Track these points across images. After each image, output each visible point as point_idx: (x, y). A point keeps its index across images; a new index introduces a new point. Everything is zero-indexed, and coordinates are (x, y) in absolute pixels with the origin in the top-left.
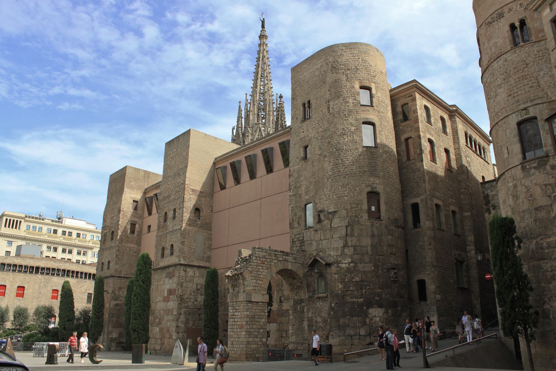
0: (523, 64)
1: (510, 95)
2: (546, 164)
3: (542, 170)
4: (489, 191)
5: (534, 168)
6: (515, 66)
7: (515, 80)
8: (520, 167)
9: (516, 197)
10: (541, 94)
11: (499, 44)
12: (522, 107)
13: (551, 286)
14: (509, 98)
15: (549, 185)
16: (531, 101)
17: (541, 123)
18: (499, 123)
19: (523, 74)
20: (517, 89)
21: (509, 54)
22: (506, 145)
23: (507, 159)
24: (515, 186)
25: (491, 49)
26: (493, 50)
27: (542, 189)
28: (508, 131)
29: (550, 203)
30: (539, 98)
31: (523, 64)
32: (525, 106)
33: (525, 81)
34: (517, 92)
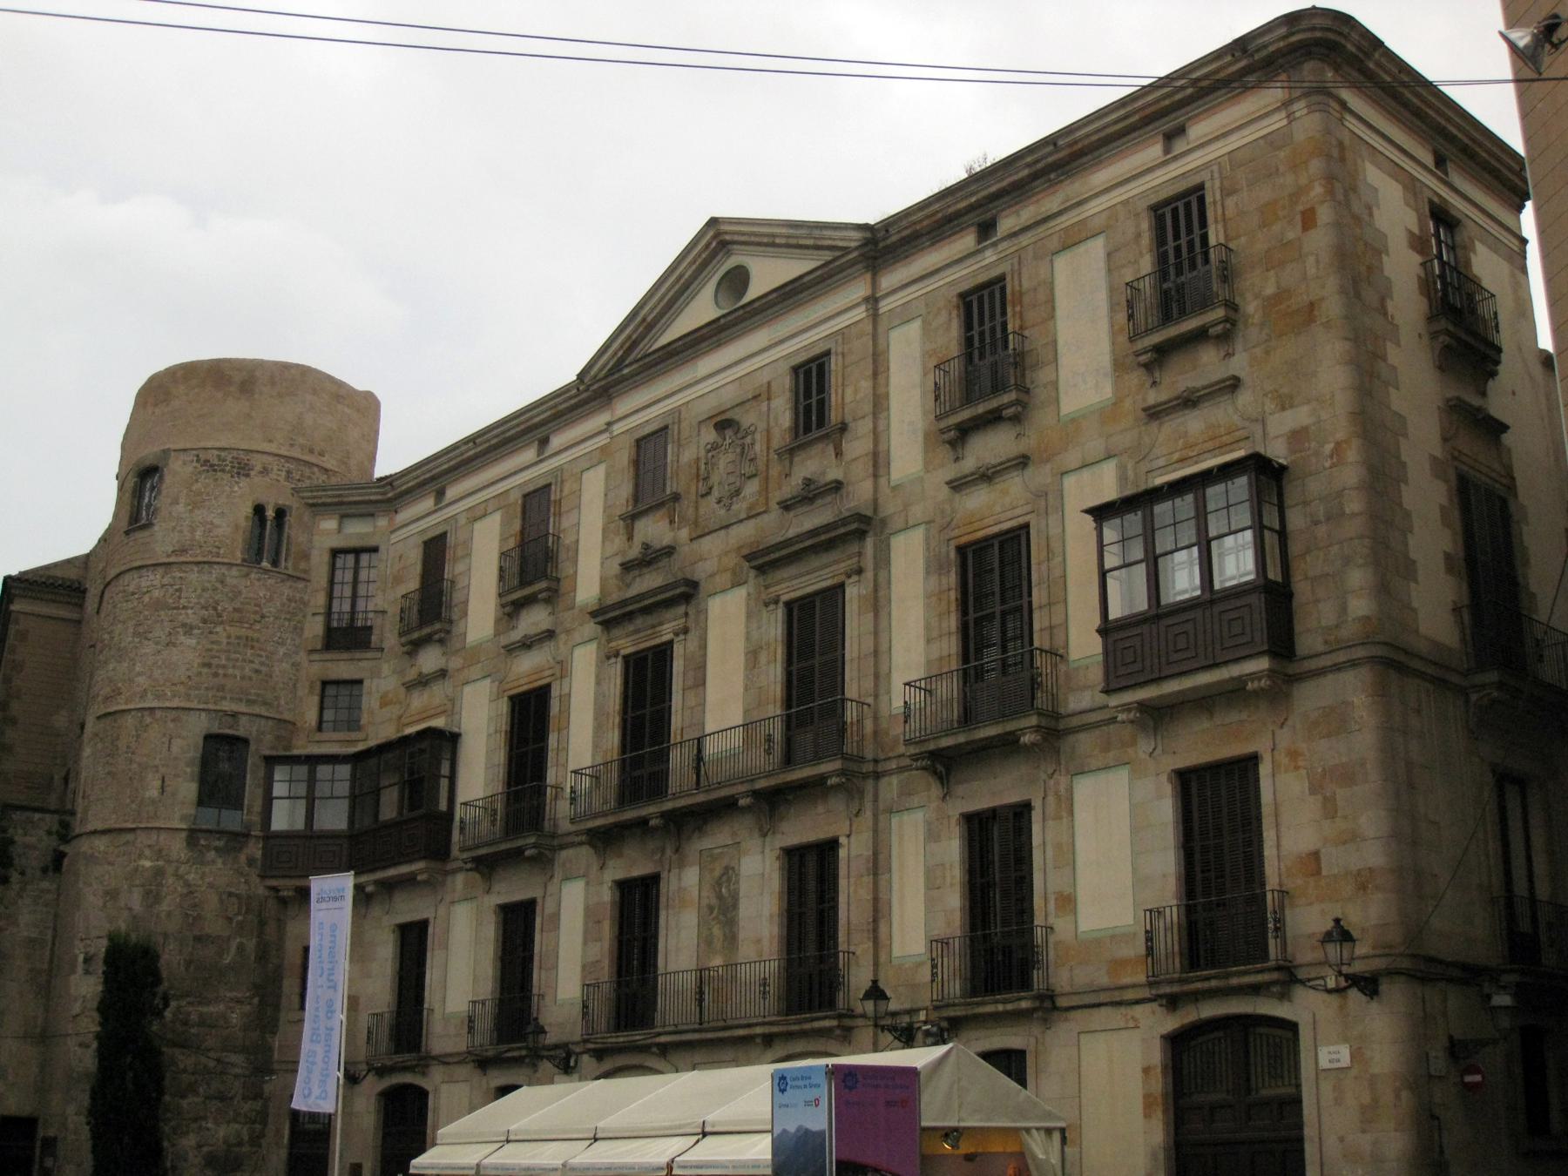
0: (255, 613)
1: (209, 665)
4: (20, 831)
6: (238, 605)
7: (229, 637)
8: (184, 835)
9: (152, 897)
11: (219, 531)
12: (227, 706)
13: (184, 1103)
14: (205, 670)
15: (238, 896)
16: (250, 702)
17: (252, 760)
19: (250, 633)
20: (228, 659)
21: (234, 571)
22: (162, 770)
23: (153, 802)
24: (159, 873)
25: (193, 531)
26: (198, 534)
27: (221, 901)
30: (265, 703)
31: (255, 613)
32: (234, 707)
33: (249, 652)
34: (224, 667)
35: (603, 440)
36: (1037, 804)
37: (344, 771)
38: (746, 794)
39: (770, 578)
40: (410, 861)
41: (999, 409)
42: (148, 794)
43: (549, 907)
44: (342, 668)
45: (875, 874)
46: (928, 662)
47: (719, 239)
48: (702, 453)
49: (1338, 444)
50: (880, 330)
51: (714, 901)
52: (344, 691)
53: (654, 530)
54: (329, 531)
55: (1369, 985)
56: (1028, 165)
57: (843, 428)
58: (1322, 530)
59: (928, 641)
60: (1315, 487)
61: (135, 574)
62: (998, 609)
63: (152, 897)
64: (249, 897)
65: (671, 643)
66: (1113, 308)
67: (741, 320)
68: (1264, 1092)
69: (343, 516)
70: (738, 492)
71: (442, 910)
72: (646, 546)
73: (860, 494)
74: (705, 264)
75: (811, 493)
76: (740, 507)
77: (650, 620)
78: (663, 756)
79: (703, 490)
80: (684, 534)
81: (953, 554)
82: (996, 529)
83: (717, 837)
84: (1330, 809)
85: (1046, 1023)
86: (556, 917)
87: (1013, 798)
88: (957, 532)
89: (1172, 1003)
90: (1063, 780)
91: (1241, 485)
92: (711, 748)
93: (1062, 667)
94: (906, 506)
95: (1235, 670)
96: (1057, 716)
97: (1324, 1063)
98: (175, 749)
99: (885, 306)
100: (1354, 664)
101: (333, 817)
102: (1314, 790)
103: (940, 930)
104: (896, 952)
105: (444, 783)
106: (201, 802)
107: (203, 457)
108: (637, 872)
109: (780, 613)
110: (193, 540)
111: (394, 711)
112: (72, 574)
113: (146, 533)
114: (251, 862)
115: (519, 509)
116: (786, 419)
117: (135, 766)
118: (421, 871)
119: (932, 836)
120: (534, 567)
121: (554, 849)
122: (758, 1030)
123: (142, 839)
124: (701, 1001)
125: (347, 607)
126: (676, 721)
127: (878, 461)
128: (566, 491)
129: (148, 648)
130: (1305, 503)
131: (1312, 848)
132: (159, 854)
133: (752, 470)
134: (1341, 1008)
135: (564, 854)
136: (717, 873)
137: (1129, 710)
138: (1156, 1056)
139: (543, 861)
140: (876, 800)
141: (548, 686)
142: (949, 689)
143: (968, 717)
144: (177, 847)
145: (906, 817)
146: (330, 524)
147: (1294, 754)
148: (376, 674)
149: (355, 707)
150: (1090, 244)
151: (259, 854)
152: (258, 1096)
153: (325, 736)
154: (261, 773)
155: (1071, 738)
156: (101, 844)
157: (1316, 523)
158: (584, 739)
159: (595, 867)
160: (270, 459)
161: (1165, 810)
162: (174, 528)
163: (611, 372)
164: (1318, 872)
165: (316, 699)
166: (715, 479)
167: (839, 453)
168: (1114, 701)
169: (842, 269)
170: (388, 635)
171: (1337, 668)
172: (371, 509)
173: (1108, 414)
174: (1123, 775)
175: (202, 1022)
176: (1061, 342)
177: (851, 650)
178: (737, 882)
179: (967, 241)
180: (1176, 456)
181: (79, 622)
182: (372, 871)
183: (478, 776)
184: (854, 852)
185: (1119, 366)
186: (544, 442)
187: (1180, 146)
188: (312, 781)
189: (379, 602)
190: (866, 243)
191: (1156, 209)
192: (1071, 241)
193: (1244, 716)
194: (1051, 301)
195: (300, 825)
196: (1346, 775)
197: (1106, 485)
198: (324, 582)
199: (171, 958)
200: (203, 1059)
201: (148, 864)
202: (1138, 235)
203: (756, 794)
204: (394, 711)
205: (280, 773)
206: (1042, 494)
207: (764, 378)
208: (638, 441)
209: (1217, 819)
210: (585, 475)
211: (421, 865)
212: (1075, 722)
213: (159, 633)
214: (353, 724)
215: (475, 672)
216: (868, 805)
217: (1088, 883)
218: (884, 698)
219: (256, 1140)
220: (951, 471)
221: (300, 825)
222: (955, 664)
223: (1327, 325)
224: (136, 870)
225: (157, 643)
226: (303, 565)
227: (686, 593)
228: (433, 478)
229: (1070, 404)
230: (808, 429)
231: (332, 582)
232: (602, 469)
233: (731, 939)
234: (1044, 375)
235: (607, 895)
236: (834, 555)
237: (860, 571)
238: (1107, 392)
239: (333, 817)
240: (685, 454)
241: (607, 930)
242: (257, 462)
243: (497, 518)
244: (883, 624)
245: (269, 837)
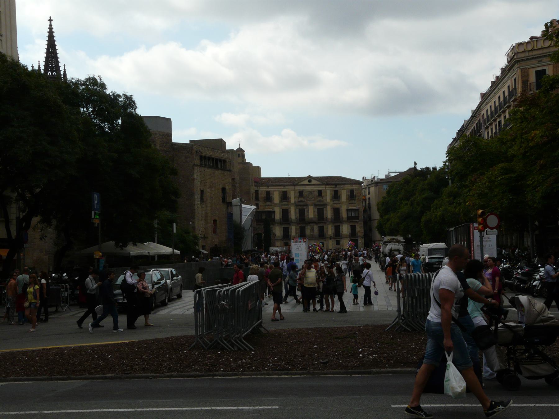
83: (312, 225)
127: (326, 200)
158: (293, 214)
184: (325, 227)
192: (343, 189)
209: (353, 228)
217: (344, 231)
227: (307, 205)
243: (278, 192)
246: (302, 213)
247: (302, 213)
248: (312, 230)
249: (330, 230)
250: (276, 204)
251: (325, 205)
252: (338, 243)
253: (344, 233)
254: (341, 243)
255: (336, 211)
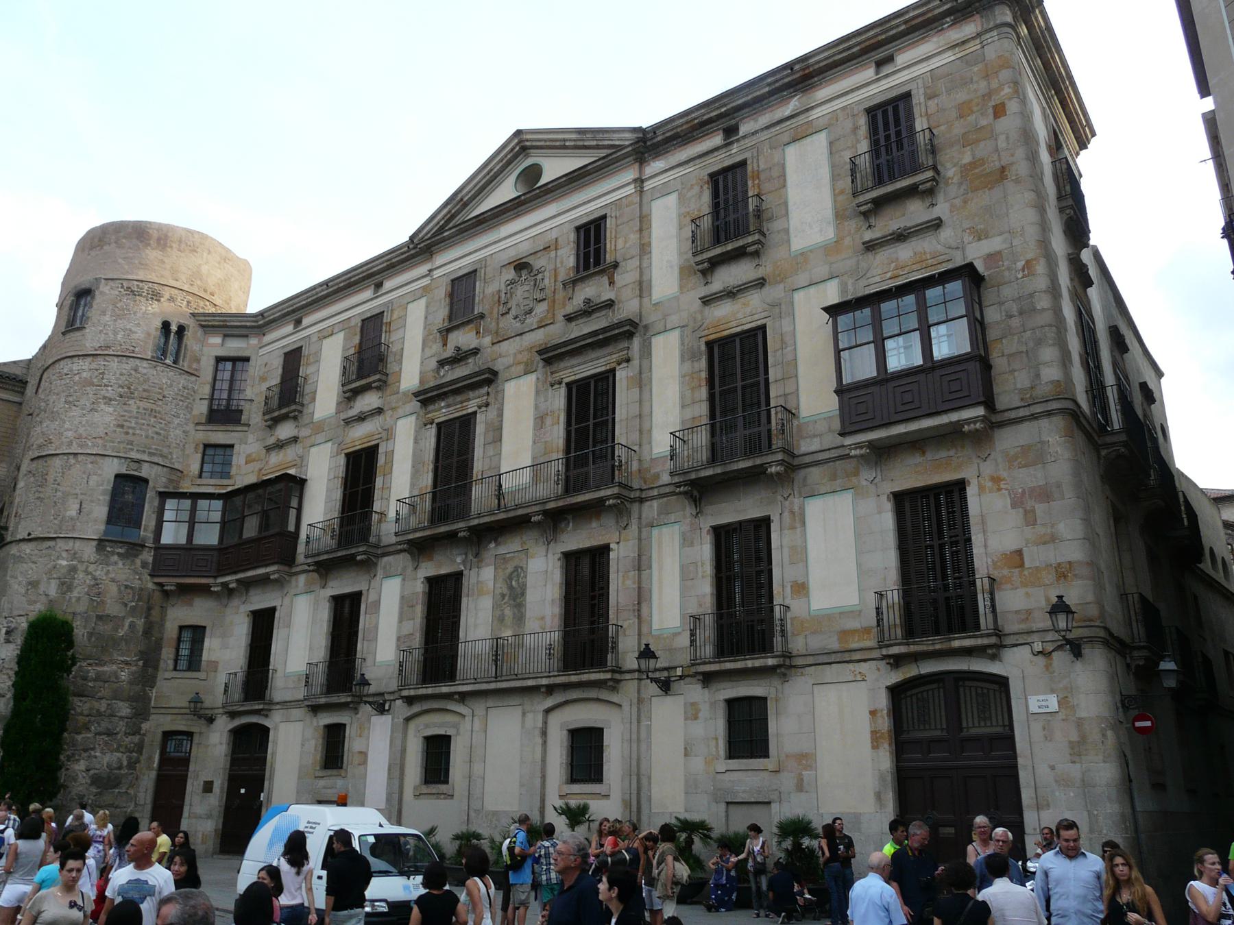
1: (122, 426)
2: (136, 556)
3: (129, 562)
5: (119, 554)
8: (94, 543)
9: (66, 586)
10: (165, 450)
13: (79, 737)
14: (119, 430)
15: (132, 588)
16: (150, 454)
17: (150, 494)
18: (80, 458)
19: (154, 407)
21: (145, 364)
22: (81, 497)
24: (73, 569)
25: (115, 333)
26: (119, 337)
27: (120, 592)
28: (94, 480)
29: (122, 614)
30: (161, 456)
33: (153, 420)
35: (426, 281)
36: (775, 519)
37: (218, 504)
38: (536, 513)
39: (555, 367)
40: (266, 566)
41: (744, 247)
42: (68, 513)
43: (372, 597)
44: (219, 436)
45: (639, 569)
46: (683, 422)
47: (522, 145)
48: (503, 287)
49: (1028, 262)
50: (645, 200)
51: (505, 591)
52: (220, 451)
53: (464, 338)
54: (216, 345)
55: (1076, 649)
56: (769, 85)
57: (616, 265)
58: (1016, 322)
59: (683, 406)
60: (1007, 292)
61: (69, 361)
62: (739, 384)
63: (66, 586)
64: (141, 589)
65: (475, 413)
66: (835, 177)
67: (537, 197)
68: (973, 731)
69: (225, 336)
70: (531, 311)
71: (287, 600)
72: (458, 349)
73: (628, 308)
74: (509, 163)
75: (589, 310)
76: (532, 321)
77: (459, 398)
78: (465, 490)
79: (502, 309)
80: (487, 340)
81: (703, 348)
82: (739, 329)
83: (511, 546)
84: (1030, 519)
85: (784, 677)
86: (377, 604)
87: (755, 513)
88: (706, 332)
89: (896, 662)
90: (797, 501)
91: (955, 287)
92: (507, 484)
93: (795, 423)
94: (665, 318)
95: (954, 417)
96: (793, 456)
97: (1034, 707)
98: (91, 483)
99: (648, 185)
100: (1048, 414)
101: (209, 536)
102: (1016, 502)
103: (694, 610)
104: (655, 626)
105: (293, 513)
106: (110, 520)
107: (125, 285)
108: (444, 571)
109: (563, 390)
110: (115, 339)
111: (257, 465)
112: (18, 371)
113: (78, 334)
114: (144, 565)
115: (358, 330)
116: (571, 261)
117: (59, 494)
118: (274, 572)
119: (686, 541)
120: (369, 365)
121: (378, 556)
122: (544, 682)
123: (61, 544)
124: (496, 661)
125: (225, 396)
126: (478, 466)
127: (643, 287)
128: (395, 316)
129: (76, 412)
130: (1001, 304)
131: (1015, 547)
132: (74, 555)
133: (542, 295)
134: (1047, 667)
135: (385, 559)
136: (510, 570)
137: (861, 448)
138: (883, 701)
139: (368, 565)
140: (640, 518)
141: (377, 446)
142: (702, 439)
143: (714, 459)
144: (89, 551)
145: (665, 529)
146: (217, 340)
147: (996, 480)
148: (243, 441)
149: (228, 463)
150: (815, 137)
151: (150, 559)
152: (137, 732)
153: (204, 481)
154: (156, 503)
155: (803, 472)
156: (27, 548)
157: (1011, 317)
158: (403, 481)
159: (410, 568)
160: (176, 291)
161: (887, 520)
162: (101, 331)
163: (434, 236)
164: (1022, 565)
165: (199, 456)
166: (512, 303)
167: (612, 283)
168: (849, 441)
169: (618, 160)
170: (254, 415)
171: (1034, 417)
172: (244, 332)
173: (830, 250)
174: (848, 497)
175: (98, 678)
176: (790, 204)
177: (620, 413)
178: (526, 577)
179: (718, 140)
180: (889, 275)
181: (20, 404)
182: (235, 573)
183: (319, 507)
184: (621, 555)
185: (840, 216)
186: (379, 285)
187: (887, 69)
188: (193, 510)
189: (249, 393)
190: (638, 141)
191: (871, 112)
193: (952, 453)
194: (783, 176)
195: (183, 540)
196: (1045, 494)
197: (832, 294)
198: (210, 379)
199: (80, 632)
200: (96, 705)
201: (64, 563)
202: (856, 129)
203: (545, 513)
204: (257, 465)
205: (171, 504)
206: (775, 305)
207: (554, 234)
208: (453, 281)
210: (410, 306)
211: (274, 568)
212: (807, 459)
213: (85, 402)
214: (226, 475)
215: (320, 438)
216: (634, 521)
218: (646, 447)
219: (132, 765)
220: (703, 291)
221: (183, 540)
222: (705, 420)
223: (1017, 181)
224: (55, 567)
225: (83, 409)
226: (195, 366)
227: (488, 379)
228: (294, 311)
229: (798, 243)
230: (587, 267)
231: (215, 379)
232: (423, 301)
233: (520, 619)
234: (777, 225)
235: (420, 587)
236: (609, 349)
237: (628, 360)
238: (830, 234)
239: (209, 536)
240: (486, 291)
241: (419, 611)
242: (167, 293)
243: (340, 337)
244: (646, 396)
245: (159, 549)
246: (454, 452)
247: (454, 452)
248: (515, 595)
249: (667, 583)
250: (319, 427)
251: (626, 332)
252: (747, 732)
253: (821, 600)
254: (784, 729)
255: (737, 370)
